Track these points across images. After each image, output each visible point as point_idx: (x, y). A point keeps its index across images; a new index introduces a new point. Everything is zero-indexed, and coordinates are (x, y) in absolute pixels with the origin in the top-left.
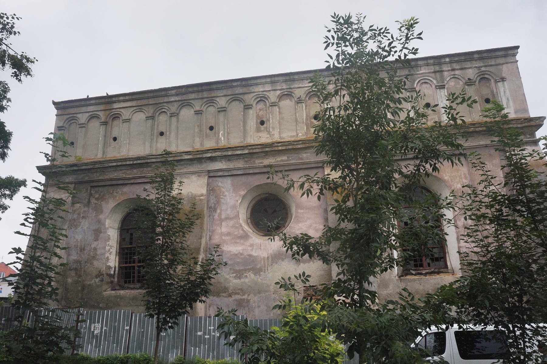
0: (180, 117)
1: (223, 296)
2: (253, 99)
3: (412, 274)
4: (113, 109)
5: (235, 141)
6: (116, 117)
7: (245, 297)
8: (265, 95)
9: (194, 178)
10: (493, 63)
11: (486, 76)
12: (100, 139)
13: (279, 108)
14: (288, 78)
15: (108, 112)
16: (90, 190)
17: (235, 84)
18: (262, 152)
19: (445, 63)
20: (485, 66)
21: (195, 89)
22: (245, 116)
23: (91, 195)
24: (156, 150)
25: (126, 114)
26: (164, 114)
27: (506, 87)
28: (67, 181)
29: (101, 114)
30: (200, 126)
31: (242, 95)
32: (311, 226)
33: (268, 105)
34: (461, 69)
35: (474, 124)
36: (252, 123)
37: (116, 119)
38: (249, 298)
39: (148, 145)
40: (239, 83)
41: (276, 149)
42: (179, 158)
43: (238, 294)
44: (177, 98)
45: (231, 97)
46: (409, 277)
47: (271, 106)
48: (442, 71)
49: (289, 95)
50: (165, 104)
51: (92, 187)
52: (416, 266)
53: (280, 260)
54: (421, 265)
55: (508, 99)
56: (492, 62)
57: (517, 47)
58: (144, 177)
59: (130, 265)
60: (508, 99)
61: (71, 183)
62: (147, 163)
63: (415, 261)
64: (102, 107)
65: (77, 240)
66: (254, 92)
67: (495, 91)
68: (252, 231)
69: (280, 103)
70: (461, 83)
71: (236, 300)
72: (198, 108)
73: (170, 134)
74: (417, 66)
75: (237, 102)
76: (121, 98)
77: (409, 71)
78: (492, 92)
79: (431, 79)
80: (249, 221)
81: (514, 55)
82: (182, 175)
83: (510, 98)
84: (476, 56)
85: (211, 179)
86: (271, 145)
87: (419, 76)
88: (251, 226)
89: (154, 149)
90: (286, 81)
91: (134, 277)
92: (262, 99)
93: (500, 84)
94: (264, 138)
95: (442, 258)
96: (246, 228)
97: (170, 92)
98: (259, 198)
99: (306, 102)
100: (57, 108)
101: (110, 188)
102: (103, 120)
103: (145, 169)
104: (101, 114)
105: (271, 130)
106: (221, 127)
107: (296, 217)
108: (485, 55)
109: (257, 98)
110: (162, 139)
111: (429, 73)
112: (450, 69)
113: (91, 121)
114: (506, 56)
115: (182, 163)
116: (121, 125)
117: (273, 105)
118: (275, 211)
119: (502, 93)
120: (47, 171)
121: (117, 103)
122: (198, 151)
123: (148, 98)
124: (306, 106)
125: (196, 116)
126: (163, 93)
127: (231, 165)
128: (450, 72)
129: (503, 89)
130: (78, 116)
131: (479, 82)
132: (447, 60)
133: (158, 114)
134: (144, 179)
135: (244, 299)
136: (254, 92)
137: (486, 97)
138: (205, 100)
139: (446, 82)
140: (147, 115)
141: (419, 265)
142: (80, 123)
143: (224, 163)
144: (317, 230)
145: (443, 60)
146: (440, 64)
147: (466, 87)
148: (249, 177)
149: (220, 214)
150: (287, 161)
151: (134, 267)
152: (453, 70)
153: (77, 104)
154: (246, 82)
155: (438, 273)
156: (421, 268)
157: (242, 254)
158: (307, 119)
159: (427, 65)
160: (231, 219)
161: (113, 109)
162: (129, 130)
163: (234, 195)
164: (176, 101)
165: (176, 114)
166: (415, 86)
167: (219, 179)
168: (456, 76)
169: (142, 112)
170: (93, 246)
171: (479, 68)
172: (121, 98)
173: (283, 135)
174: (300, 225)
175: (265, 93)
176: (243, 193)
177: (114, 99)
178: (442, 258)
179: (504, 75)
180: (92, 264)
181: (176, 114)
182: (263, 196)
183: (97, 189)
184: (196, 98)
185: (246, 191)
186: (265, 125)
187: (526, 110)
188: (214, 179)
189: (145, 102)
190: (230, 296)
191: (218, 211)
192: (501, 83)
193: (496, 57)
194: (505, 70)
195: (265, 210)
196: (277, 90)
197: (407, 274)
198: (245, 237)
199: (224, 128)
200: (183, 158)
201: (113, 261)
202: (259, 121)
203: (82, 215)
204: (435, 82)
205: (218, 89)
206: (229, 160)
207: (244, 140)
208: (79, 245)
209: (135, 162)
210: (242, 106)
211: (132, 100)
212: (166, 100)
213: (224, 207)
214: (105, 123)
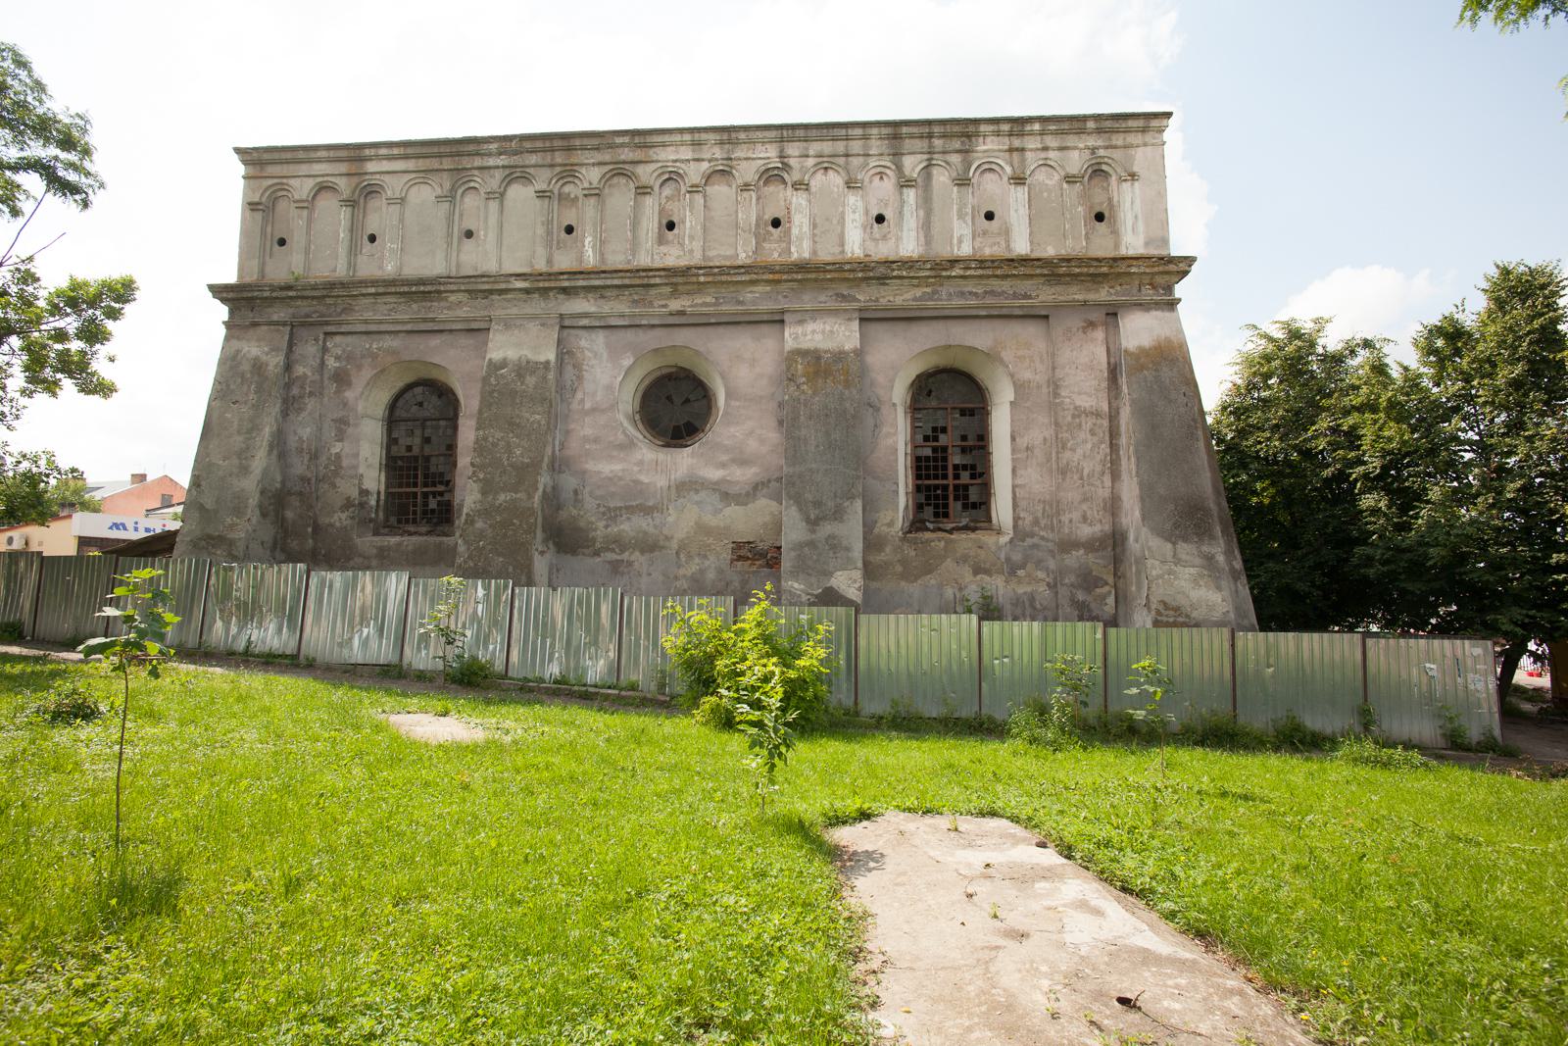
0: (505, 203)
1: (584, 554)
2: (655, 174)
3: (928, 529)
4: (366, 173)
5: (617, 259)
6: (371, 191)
7: (625, 556)
8: (679, 168)
9: (533, 328)
10: (1120, 143)
11: (1104, 167)
12: (342, 235)
13: (705, 197)
14: (725, 137)
15: (355, 180)
16: (324, 342)
17: (619, 140)
18: (666, 284)
19: (1031, 133)
20: (1107, 148)
21: (539, 144)
22: (637, 208)
23: (325, 350)
24: (458, 265)
25: (394, 186)
26: (471, 191)
27: (1137, 191)
28: (275, 318)
29: (342, 183)
30: (549, 223)
31: (632, 166)
32: (751, 433)
33: (683, 190)
34: (1061, 149)
35: (1069, 260)
36: (650, 224)
37: (374, 195)
38: (632, 558)
39: (440, 256)
40: (626, 139)
41: (694, 279)
42: (503, 286)
43: (613, 550)
44: (502, 161)
45: (611, 167)
46: (920, 535)
47: (689, 192)
48: (1023, 150)
49: (724, 173)
50: (476, 172)
51: (326, 334)
53: (692, 493)
54: (946, 515)
55: (1136, 217)
56: (1118, 140)
57: (1168, 115)
58: (433, 320)
59: (408, 490)
60: (1136, 217)
61: (284, 324)
62: (439, 292)
63: (936, 506)
64: (343, 168)
65: (300, 438)
66: (657, 161)
67: (1115, 199)
68: (641, 437)
69: (707, 188)
70: (1057, 177)
71: (609, 562)
72: (544, 187)
73: (486, 236)
74: (977, 134)
75: (623, 180)
76: (383, 151)
77: (962, 142)
78: (1110, 200)
79: (999, 161)
80: (637, 417)
81: (1161, 131)
82: (508, 324)
83: (1140, 216)
84: (1091, 125)
85: (566, 332)
86: (686, 271)
87: (980, 155)
88: (640, 426)
89: (454, 264)
90: (722, 143)
91: (415, 513)
92: (672, 177)
93: (1126, 186)
94: (672, 256)
95: (984, 503)
96: (631, 430)
97: (486, 146)
98: (658, 374)
99: (758, 189)
100: (245, 162)
101: (364, 337)
102: (345, 197)
103: (435, 304)
104: (342, 183)
105: (687, 242)
106: (589, 228)
107: (726, 413)
108: (1108, 124)
109: (663, 173)
110: (468, 244)
111: (1000, 151)
112: (1040, 146)
113: (318, 198)
114: (1144, 130)
115: (509, 296)
116: (384, 209)
117: (694, 189)
118: (687, 401)
119: (1128, 204)
120: (231, 295)
121: (374, 162)
122: (541, 275)
123: (440, 156)
124: (758, 199)
125: (538, 202)
126: (471, 148)
127: (606, 307)
128: (1038, 152)
129: (1130, 195)
130: (292, 182)
131: (1090, 178)
132: (1037, 127)
133: (460, 191)
134: (431, 324)
136: (657, 161)
137: (1098, 209)
138: (558, 169)
139: (1028, 173)
140: (439, 191)
141: (942, 513)
142: (297, 197)
143: (592, 301)
144: (762, 441)
145: (1028, 128)
146: (1021, 134)
147: (1065, 185)
148: (640, 332)
149: (582, 401)
150: (715, 305)
151: (415, 495)
152: (1045, 149)
153: (289, 155)
154: (642, 139)
155: (974, 529)
156: (945, 520)
157: (620, 479)
158: (757, 225)
159: (998, 134)
160: (603, 411)
161: (366, 173)
162: (402, 220)
163: (609, 365)
164: (497, 167)
165: (497, 195)
166: (971, 174)
167: (581, 332)
168: (1049, 162)
169: (422, 186)
170: (334, 451)
171: (1093, 150)
172: (383, 151)
173: (711, 254)
174: (732, 430)
175: (678, 164)
176: (627, 362)
177: (367, 152)
178: (984, 503)
179: (1135, 169)
180: (334, 486)
181: (497, 195)
182: (665, 371)
183: (338, 339)
184: (540, 162)
185: (632, 360)
186: (676, 231)
187: (1165, 241)
188: (573, 332)
189: (434, 164)
190: (597, 554)
191: (579, 395)
192: (1129, 183)
193: (1127, 131)
194: (1140, 158)
195: (669, 398)
196: (703, 160)
197: (918, 530)
198: (629, 445)
199: (595, 231)
200: (511, 286)
201: (373, 479)
202: (664, 222)
203: (308, 390)
204: (1008, 170)
205: (584, 148)
206: (602, 297)
207: (634, 255)
208: (305, 446)
209: (414, 289)
210: (632, 185)
211: (406, 157)
212: (478, 162)
213: (588, 386)
214: (351, 203)
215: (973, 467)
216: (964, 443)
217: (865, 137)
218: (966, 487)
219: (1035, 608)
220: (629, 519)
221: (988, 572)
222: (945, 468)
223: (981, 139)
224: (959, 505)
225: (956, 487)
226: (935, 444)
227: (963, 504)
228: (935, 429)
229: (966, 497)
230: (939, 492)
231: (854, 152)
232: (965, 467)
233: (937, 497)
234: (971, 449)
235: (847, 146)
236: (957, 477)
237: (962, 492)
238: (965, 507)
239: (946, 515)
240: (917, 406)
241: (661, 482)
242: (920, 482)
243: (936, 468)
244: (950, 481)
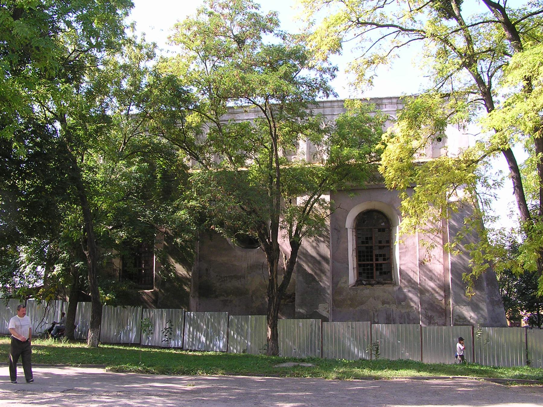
43: (223, 295)
52: (368, 277)
54: (372, 277)
63: (368, 273)
71: (222, 301)
135: (228, 300)
155: (383, 284)
159: (391, 103)
190: (216, 297)
215: (384, 255)
216: (380, 245)
217: (332, 107)
218: (381, 265)
219: (409, 319)
220: (230, 281)
221: (388, 303)
222: (372, 256)
223: (384, 106)
224: (378, 273)
225: (377, 265)
226: (367, 245)
227: (380, 272)
228: (367, 238)
229: (381, 269)
230: (369, 267)
231: (327, 113)
232: (381, 255)
233: (368, 269)
234: (384, 247)
235: (324, 111)
236: (377, 260)
237: (379, 267)
238: (381, 273)
239: (372, 277)
240: (359, 228)
241: (245, 265)
242: (360, 263)
243: (367, 256)
244: (374, 262)
